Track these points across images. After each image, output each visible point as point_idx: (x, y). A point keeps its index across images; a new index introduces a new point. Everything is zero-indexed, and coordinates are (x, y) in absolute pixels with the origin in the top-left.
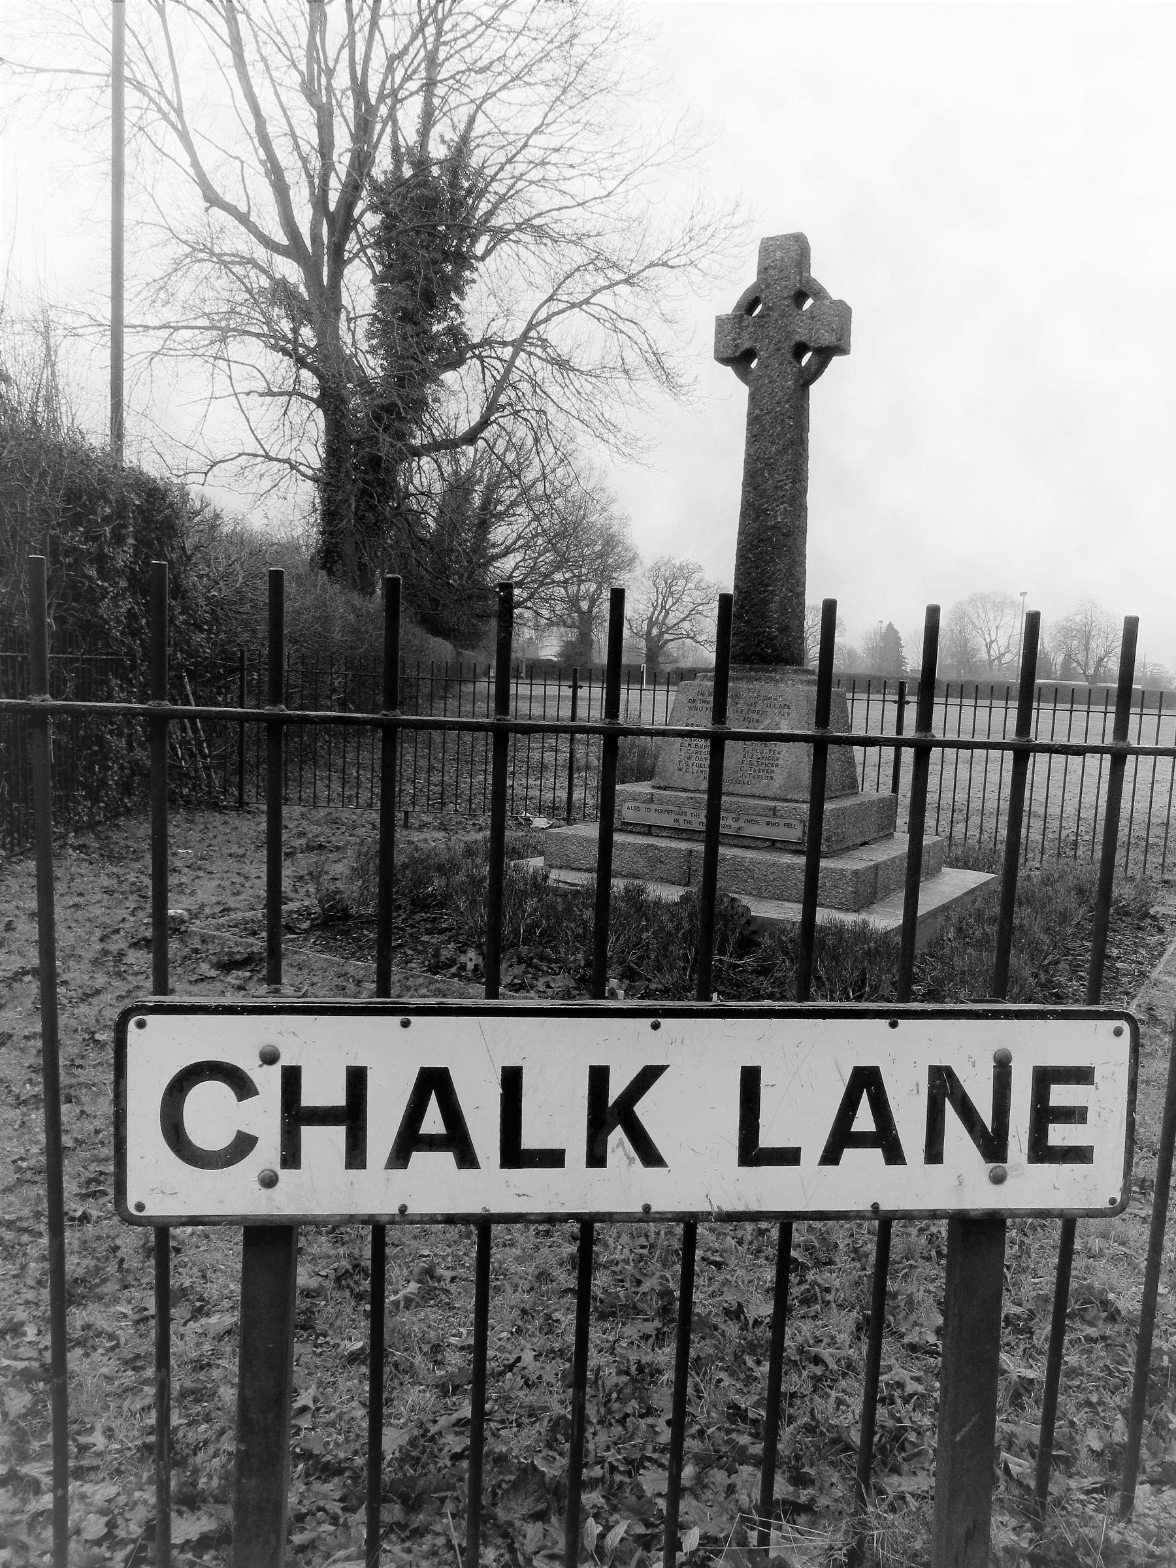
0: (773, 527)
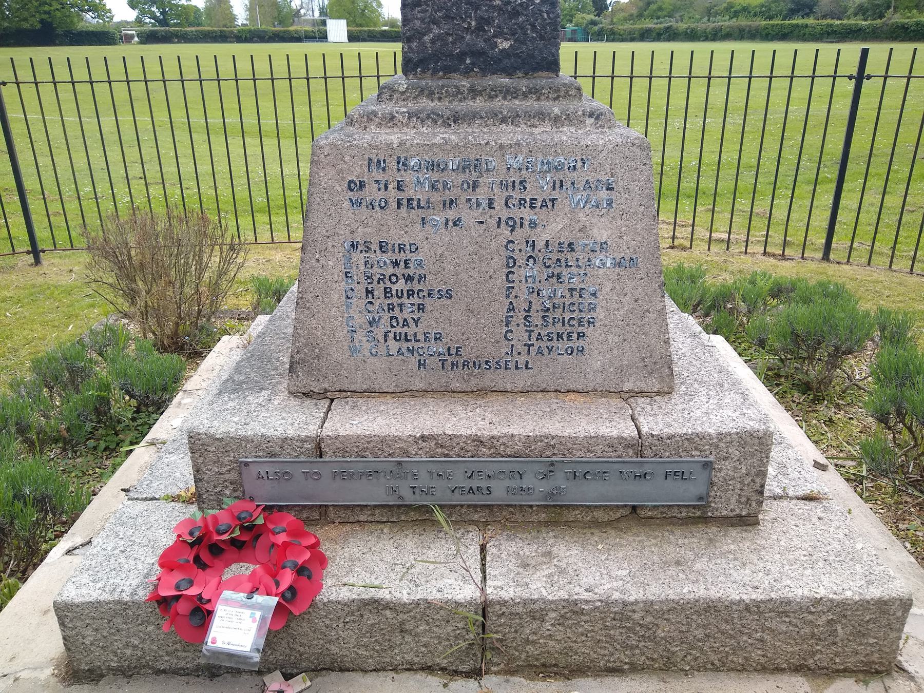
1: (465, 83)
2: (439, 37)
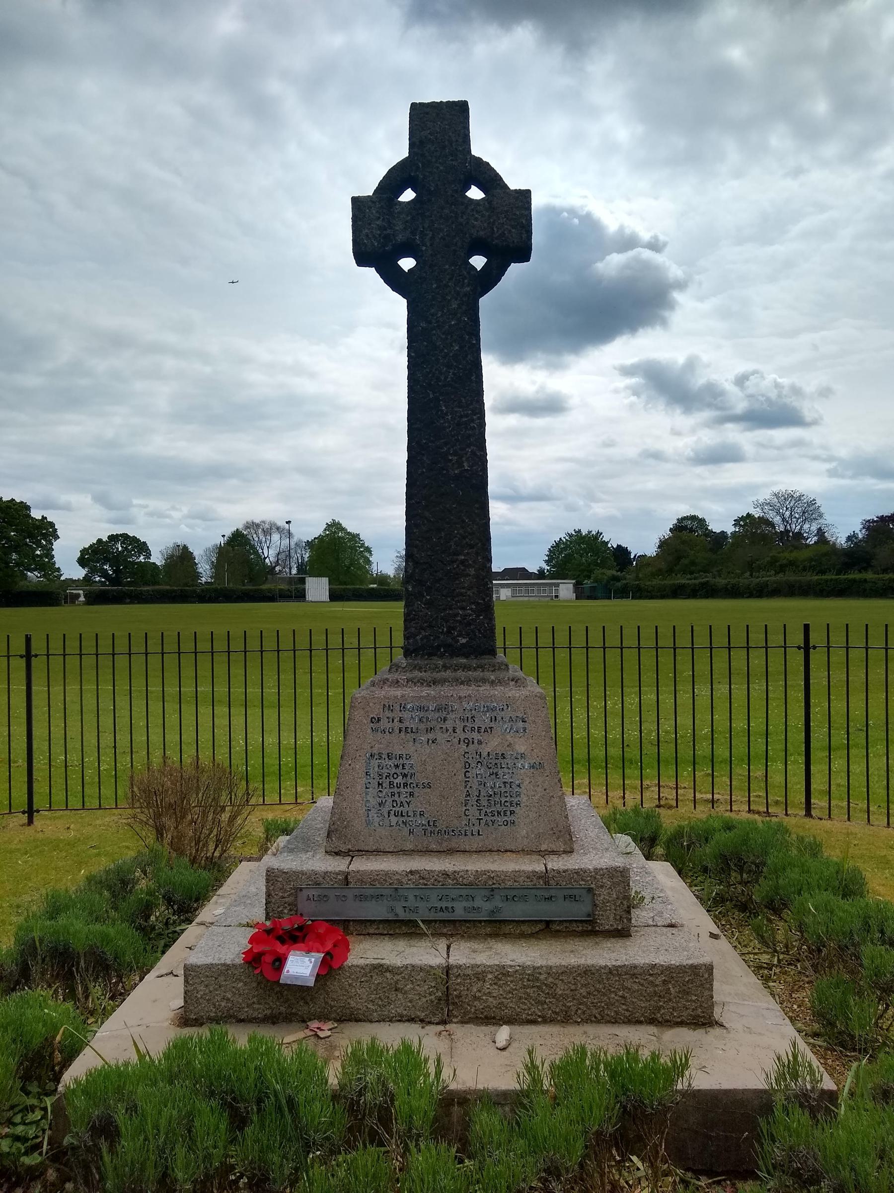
1: (441, 662)
2: (426, 637)
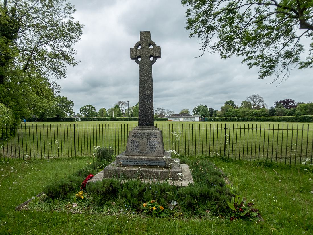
0: (147, 96)
1: (144, 127)
2: (142, 122)
